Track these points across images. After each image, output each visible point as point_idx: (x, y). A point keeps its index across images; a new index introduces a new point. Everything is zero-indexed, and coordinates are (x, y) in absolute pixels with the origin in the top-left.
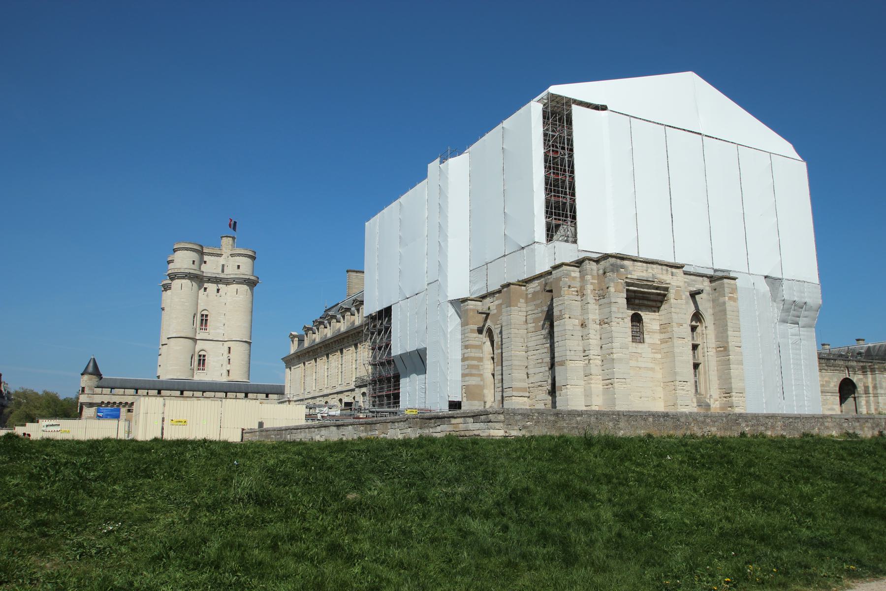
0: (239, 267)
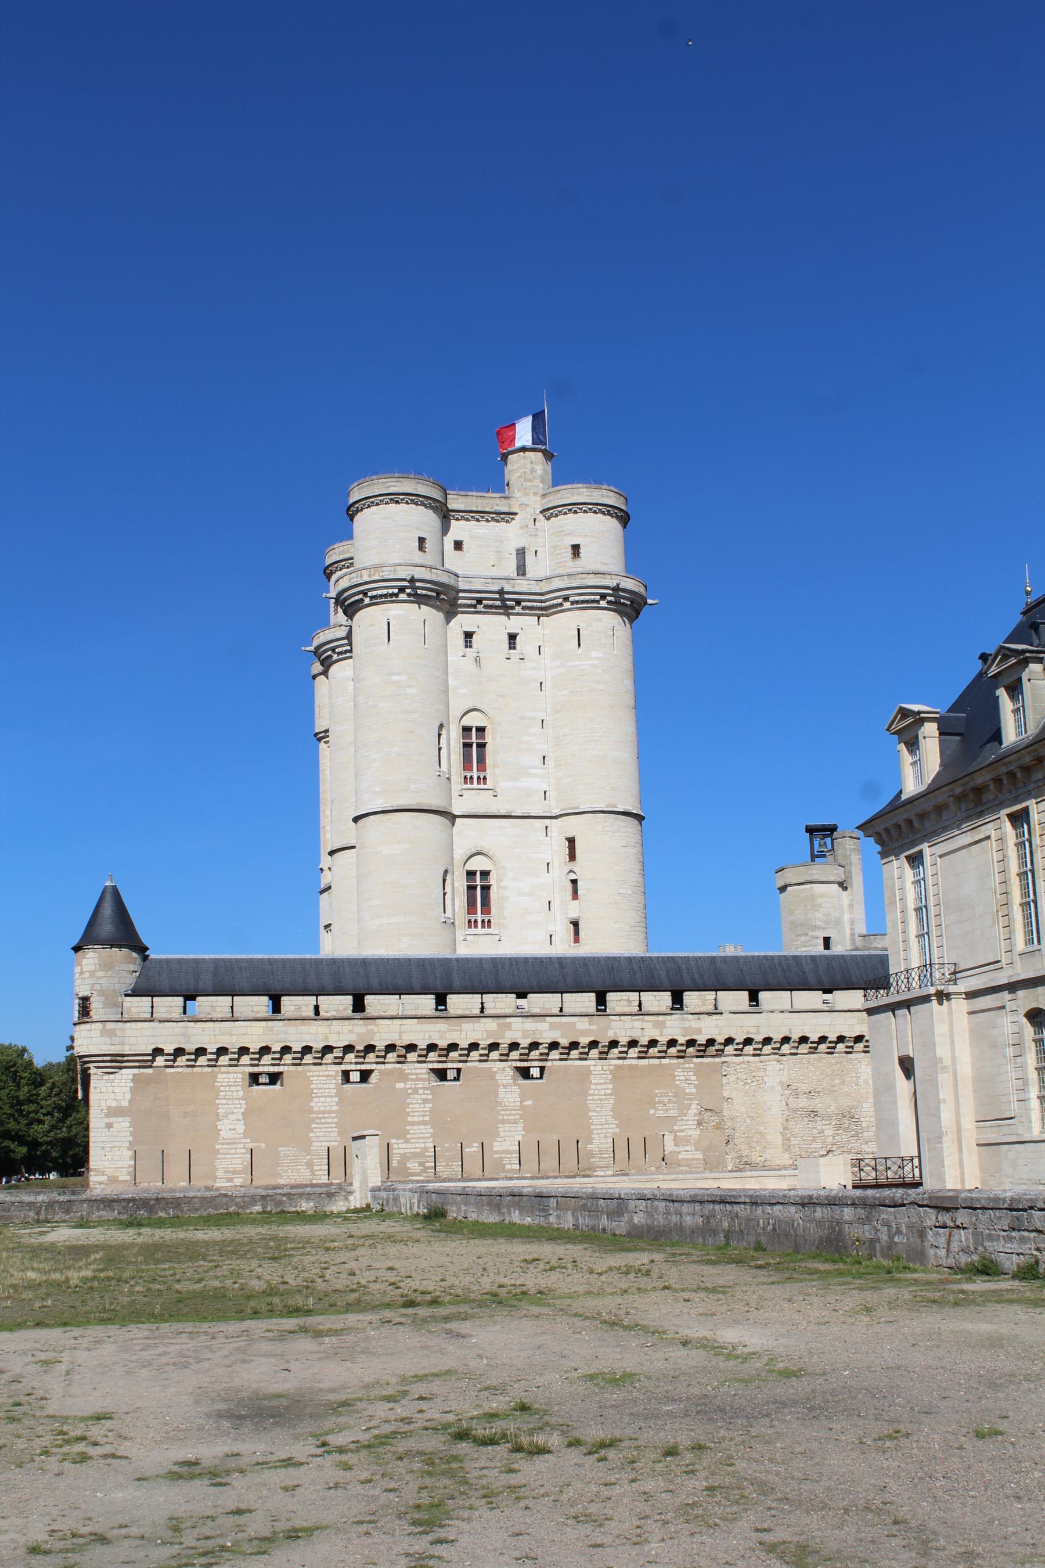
0: (576, 549)
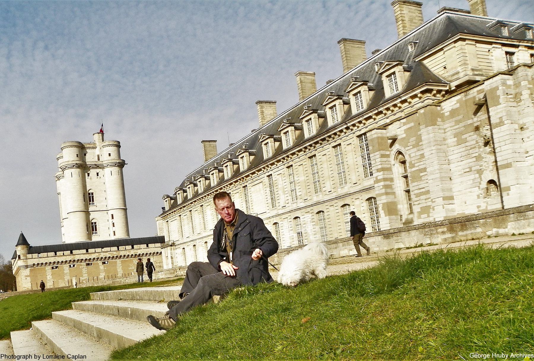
0: (110, 155)
